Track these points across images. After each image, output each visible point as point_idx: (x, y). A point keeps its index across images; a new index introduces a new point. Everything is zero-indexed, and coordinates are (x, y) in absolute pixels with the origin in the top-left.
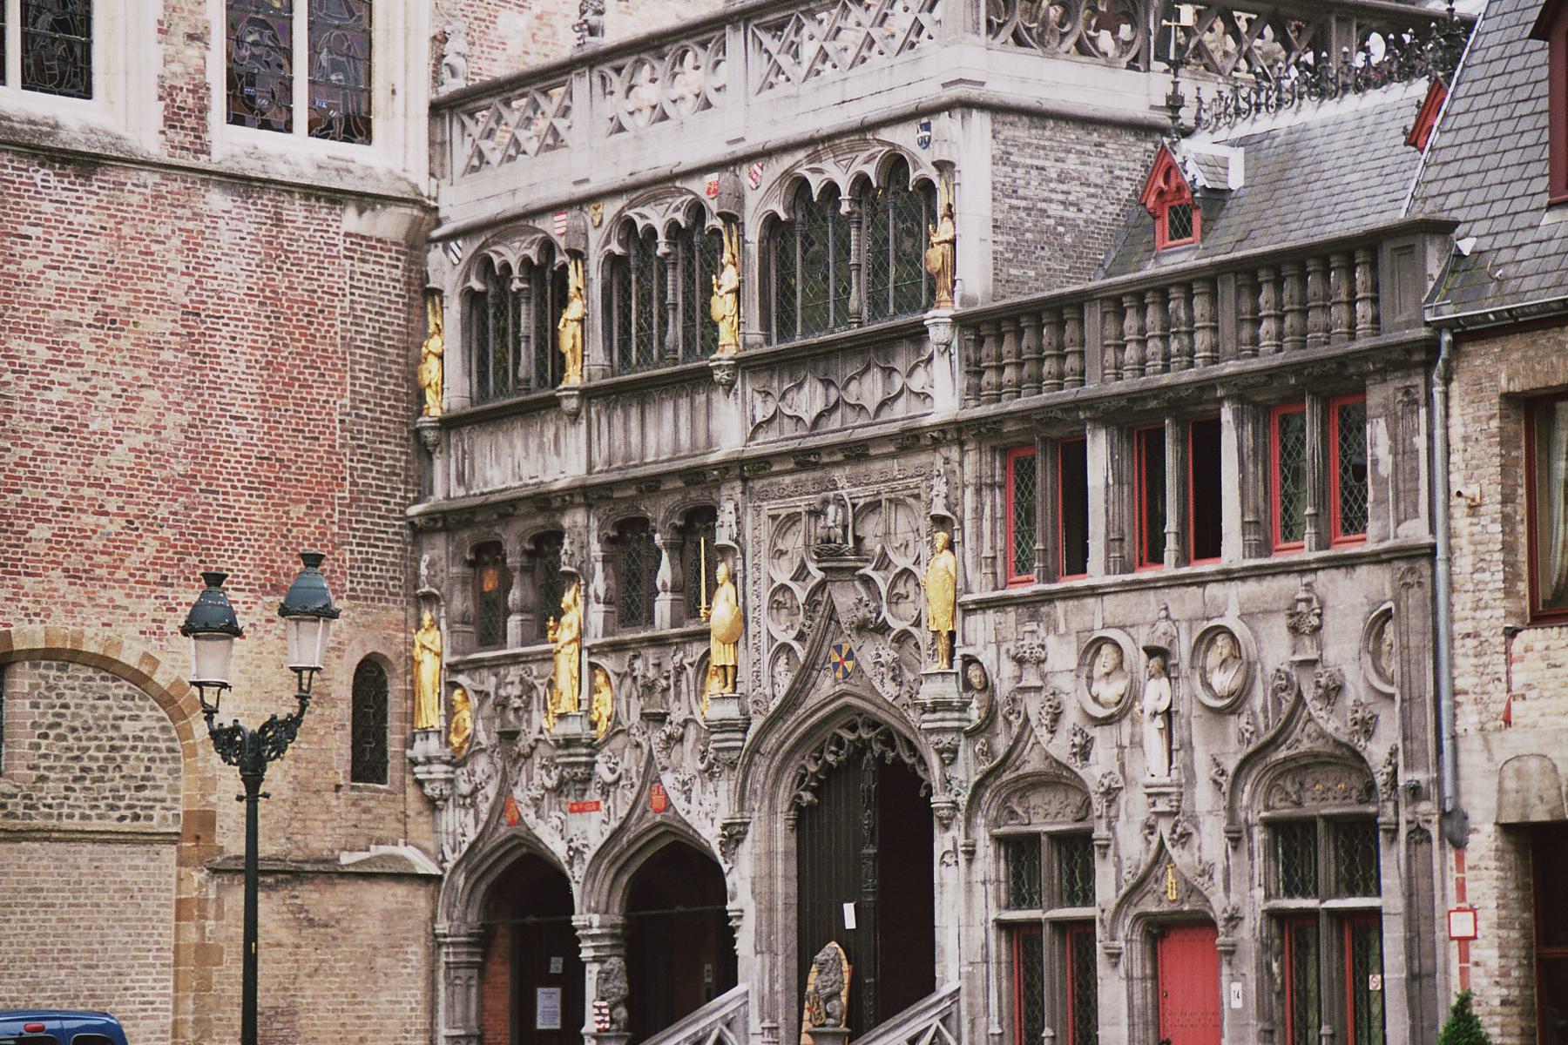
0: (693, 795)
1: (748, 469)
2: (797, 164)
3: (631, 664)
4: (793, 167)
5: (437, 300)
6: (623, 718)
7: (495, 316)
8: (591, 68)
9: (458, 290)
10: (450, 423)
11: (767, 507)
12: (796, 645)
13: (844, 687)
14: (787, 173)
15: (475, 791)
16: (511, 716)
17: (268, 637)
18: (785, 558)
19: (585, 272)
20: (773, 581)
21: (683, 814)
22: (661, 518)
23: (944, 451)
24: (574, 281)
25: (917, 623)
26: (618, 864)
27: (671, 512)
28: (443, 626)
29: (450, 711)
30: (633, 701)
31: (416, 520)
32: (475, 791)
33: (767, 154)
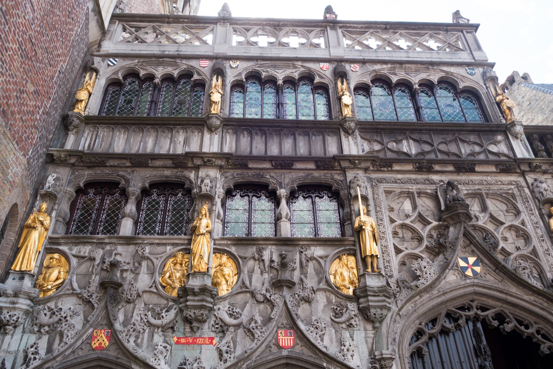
0: (326, 338)
2: (383, 69)
4: (380, 70)
6: (248, 283)
8: (230, 24)
9: (107, 76)
11: (382, 187)
12: (424, 256)
13: (476, 281)
14: (375, 71)
16: (118, 274)
18: (392, 213)
19: (223, 81)
21: (324, 350)
24: (216, 82)
25: (534, 252)
27: (293, 182)
28: (54, 214)
30: (256, 276)
31: (55, 153)
33: (363, 62)
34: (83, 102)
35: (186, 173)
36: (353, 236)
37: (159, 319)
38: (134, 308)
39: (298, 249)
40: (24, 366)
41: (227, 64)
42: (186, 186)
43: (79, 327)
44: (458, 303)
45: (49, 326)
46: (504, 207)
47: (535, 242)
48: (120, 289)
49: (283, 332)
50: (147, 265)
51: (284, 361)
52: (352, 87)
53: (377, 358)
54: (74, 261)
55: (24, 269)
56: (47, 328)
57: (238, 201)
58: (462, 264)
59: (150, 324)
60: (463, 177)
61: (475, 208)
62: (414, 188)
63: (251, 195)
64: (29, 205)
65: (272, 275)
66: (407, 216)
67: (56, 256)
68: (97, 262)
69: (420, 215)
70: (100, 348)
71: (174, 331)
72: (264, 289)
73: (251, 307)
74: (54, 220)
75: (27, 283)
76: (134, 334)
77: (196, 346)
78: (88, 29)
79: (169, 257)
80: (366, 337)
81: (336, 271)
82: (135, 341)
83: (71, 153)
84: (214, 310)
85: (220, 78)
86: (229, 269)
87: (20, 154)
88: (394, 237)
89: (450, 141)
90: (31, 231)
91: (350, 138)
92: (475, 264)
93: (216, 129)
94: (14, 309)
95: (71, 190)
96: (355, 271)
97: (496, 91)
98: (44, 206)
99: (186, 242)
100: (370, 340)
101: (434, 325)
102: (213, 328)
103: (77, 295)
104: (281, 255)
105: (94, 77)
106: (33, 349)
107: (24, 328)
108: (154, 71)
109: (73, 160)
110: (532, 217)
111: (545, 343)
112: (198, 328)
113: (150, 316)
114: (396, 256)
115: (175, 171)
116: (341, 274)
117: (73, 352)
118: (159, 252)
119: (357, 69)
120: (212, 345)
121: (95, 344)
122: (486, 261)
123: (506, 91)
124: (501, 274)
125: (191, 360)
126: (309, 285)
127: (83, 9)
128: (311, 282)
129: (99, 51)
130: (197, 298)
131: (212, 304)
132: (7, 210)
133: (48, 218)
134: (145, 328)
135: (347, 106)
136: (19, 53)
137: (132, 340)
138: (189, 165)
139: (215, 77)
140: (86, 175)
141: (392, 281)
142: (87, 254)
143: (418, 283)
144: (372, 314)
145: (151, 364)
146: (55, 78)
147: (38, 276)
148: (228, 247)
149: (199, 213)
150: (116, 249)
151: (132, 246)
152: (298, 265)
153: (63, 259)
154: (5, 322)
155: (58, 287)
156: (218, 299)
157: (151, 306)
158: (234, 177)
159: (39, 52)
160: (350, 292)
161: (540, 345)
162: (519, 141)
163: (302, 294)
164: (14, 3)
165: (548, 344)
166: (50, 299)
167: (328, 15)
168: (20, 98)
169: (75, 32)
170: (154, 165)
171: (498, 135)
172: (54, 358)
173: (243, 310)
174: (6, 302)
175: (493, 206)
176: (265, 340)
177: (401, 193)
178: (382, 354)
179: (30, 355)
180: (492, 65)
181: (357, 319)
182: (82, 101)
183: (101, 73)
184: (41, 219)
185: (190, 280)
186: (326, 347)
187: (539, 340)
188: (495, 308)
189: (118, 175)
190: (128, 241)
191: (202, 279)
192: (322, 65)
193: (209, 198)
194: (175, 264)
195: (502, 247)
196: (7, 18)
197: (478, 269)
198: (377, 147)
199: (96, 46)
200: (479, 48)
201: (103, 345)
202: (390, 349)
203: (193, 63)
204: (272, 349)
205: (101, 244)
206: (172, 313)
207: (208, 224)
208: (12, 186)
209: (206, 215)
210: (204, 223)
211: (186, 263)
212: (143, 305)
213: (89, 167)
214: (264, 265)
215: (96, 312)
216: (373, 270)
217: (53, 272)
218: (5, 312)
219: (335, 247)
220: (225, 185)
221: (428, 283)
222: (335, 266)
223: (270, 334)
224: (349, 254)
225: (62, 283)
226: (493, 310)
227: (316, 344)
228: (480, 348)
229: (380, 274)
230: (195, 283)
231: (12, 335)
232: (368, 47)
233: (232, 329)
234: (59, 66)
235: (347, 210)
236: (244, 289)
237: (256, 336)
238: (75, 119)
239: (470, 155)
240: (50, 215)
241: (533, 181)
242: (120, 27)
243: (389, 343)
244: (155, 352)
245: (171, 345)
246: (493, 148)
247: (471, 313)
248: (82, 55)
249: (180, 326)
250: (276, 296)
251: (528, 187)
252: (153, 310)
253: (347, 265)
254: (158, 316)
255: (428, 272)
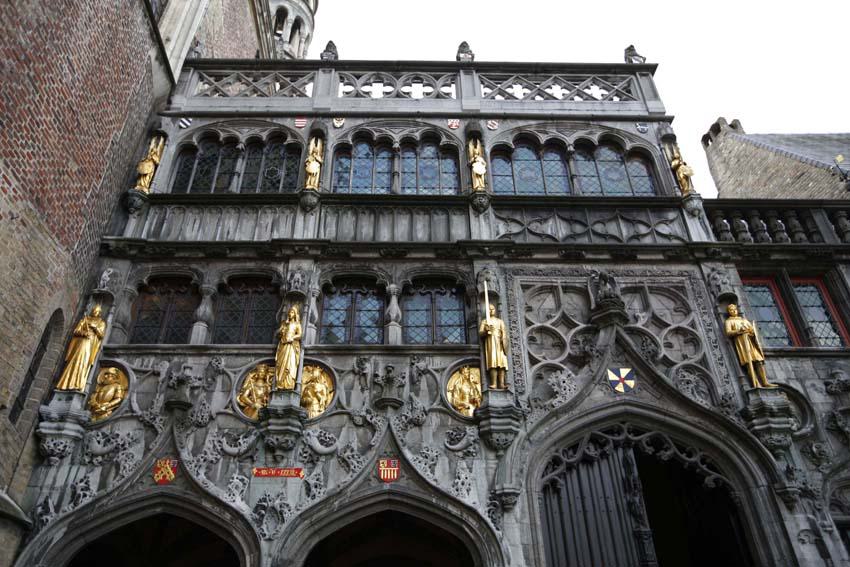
0: (438, 469)
1: (508, 251)
2: (530, 125)
3: (361, 363)
5: (162, 139)
6: (344, 403)
7: (199, 164)
9: (179, 140)
10: (157, 200)
11: (518, 280)
13: (627, 398)
14: (519, 128)
15: (116, 450)
16: (188, 392)
17: (18, 236)
19: (324, 145)
20: (529, 323)
21: (434, 483)
22: (398, 275)
23: (710, 264)
24: (314, 146)
25: (704, 361)
26: (316, 527)
27: (407, 274)
29: (94, 384)
30: (355, 394)
31: (112, 243)
32: (116, 450)
34: (148, 177)
35: (274, 265)
36: (478, 343)
37: (236, 446)
38: (207, 433)
39: (408, 360)
40: (72, 504)
41: (328, 123)
42: (273, 281)
43: (138, 457)
44: (605, 425)
45: (103, 456)
46: (672, 305)
47: (706, 348)
48: (191, 411)
49: (386, 462)
50: (223, 381)
51: (386, 497)
52: (488, 150)
53: (498, 492)
54: (134, 377)
55: (71, 387)
56: (100, 459)
57: (339, 299)
58: (612, 376)
59: (224, 453)
60: (621, 268)
61: (633, 305)
62: (559, 281)
63: (354, 291)
64: (79, 308)
65: (375, 392)
66: (549, 317)
67: (112, 370)
68: (161, 379)
69: (564, 316)
70: (164, 481)
71: (253, 461)
72: (364, 409)
73: (348, 431)
74: (110, 326)
75: (76, 405)
76: (205, 464)
77: (279, 479)
78: (151, 83)
79: (250, 370)
80: (487, 468)
81: (455, 386)
82: (205, 474)
83: (134, 243)
84: (303, 435)
85: (319, 141)
86: (322, 386)
87: (61, 250)
88: (529, 344)
89: (610, 220)
90: (81, 342)
91: (481, 216)
92: (628, 377)
93: (312, 207)
94: (60, 436)
95: (132, 288)
96: (479, 387)
97: (673, 153)
98: (98, 309)
99: (271, 352)
100: (492, 472)
101: (575, 453)
102: (301, 458)
103: (137, 418)
104: (386, 368)
105: (161, 143)
106: (82, 484)
107: (72, 459)
108: (237, 133)
109: (133, 252)
110: (705, 317)
111: (710, 475)
112: (283, 457)
113: (225, 443)
114: (531, 367)
115: (260, 263)
116: (460, 390)
117: (132, 486)
118: (239, 364)
119: (496, 127)
120: (298, 479)
121: (158, 477)
122: (642, 373)
123: (710, 143)
124: (660, 390)
125: (273, 496)
126: (420, 405)
127: (142, 60)
128: (423, 402)
129: (169, 109)
130: (281, 421)
131: (300, 428)
132: (47, 318)
133: (103, 324)
134: (219, 456)
135: (479, 176)
136: (55, 126)
137: (202, 472)
138: (278, 255)
139: (313, 140)
140: (150, 268)
141: (523, 399)
142: (149, 368)
143: (554, 402)
144: (495, 440)
145: (224, 500)
146: (107, 151)
147: (90, 394)
148: (322, 358)
149: (287, 315)
150: (186, 362)
151: (204, 358)
152: (407, 380)
153: (121, 373)
154: (49, 452)
155: (115, 408)
156: (307, 422)
157: (226, 431)
158: (334, 270)
159: (83, 121)
160: (471, 413)
161: (704, 477)
162: (696, 219)
163: (410, 415)
164: (45, 64)
165: (715, 475)
166: (105, 423)
167: (462, 55)
168: (60, 181)
169: (132, 90)
170: (233, 255)
171: (670, 211)
172: (108, 495)
173: (338, 437)
174: (50, 428)
175: (657, 304)
176: (363, 471)
177: (542, 288)
178: (503, 489)
179: (79, 492)
180: (670, 120)
181: (477, 446)
182: (146, 175)
183: (170, 138)
184: (93, 325)
185: (273, 399)
186: (436, 480)
187: (704, 471)
188: (650, 431)
189: (190, 269)
190: (200, 351)
191: (287, 398)
192: (450, 121)
193: (299, 298)
194: (257, 379)
195: (665, 356)
196: (37, 85)
197: (631, 383)
198: (515, 229)
199: (165, 103)
200: (656, 96)
201: (168, 478)
202: (514, 480)
203: (287, 122)
204: (371, 483)
205: (166, 355)
206: (253, 438)
207: (297, 329)
208: (52, 289)
209: (295, 318)
210: (292, 330)
211: (270, 377)
212: (216, 430)
213: (154, 260)
214: (366, 380)
215: (159, 439)
216: (499, 386)
217: (109, 390)
218: (49, 439)
219: (455, 358)
220: (322, 280)
221: (567, 401)
222: (456, 380)
223: (369, 463)
224: (471, 366)
225: (120, 403)
226: (648, 434)
227: (425, 477)
228: (629, 481)
229: (507, 391)
230: (278, 403)
231: (59, 468)
232: (511, 97)
233: (323, 459)
234: (112, 136)
235: (473, 310)
236: (339, 410)
237: (352, 467)
238: (136, 199)
239: (633, 237)
240: (105, 320)
241: (709, 271)
242: (196, 77)
243: (514, 474)
244: (230, 486)
245: (250, 479)
246: (664, 229)
247: (621, 437)
248: (146, 116)
249: (262, 458)
250: (379, 418)
251: (704, 279)
252: (227, 435)
253: (469, 380)
254: (234, 442)
255: (568, 388)
